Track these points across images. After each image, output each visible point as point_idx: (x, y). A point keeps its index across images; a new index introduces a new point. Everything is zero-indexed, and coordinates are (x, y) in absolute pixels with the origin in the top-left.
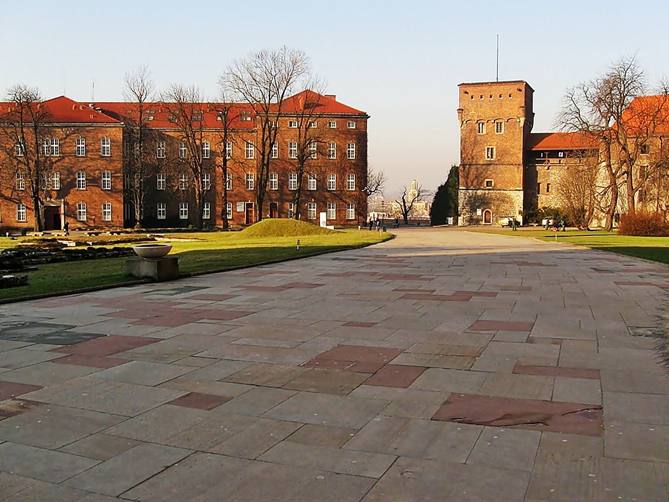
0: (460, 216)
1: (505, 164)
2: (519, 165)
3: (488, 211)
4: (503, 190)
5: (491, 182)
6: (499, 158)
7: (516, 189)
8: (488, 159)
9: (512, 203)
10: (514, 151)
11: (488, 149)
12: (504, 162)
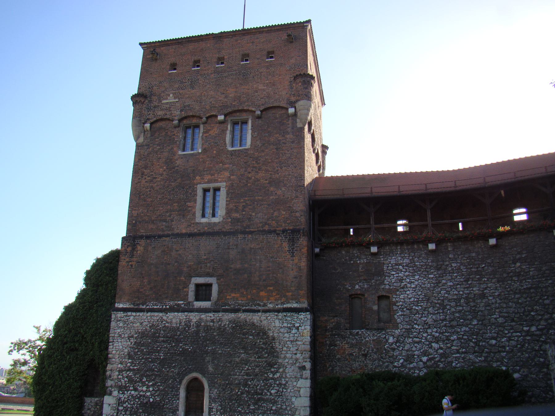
0: (110, 394)
1: (251, 233)
3: (196, 379)
4: (245, 311)
5: (210, 285)
6: (236, 215)
7: (289, 305)
8: (204, 220)
10: (279, 192)
11: (206, 191)
12: (248, 227)
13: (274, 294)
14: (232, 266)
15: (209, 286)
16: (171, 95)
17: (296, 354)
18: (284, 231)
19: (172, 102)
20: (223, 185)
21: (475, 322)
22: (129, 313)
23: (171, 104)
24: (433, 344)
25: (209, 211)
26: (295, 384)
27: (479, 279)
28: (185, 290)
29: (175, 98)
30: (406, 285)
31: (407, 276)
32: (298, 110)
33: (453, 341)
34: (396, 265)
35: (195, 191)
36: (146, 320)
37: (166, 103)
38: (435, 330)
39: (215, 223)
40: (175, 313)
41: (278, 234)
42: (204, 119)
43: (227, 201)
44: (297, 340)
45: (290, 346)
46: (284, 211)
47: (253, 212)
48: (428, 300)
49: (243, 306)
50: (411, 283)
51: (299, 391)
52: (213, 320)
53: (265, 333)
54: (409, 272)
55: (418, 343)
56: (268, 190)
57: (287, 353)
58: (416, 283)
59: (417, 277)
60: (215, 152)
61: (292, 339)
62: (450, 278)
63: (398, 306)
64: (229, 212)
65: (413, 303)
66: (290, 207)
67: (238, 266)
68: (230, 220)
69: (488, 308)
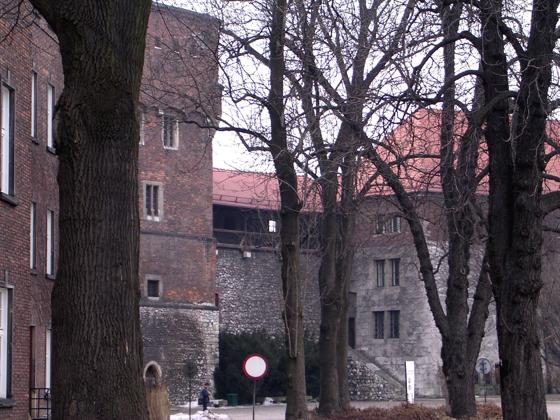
1: (183, 236)
2: (209, 240)
6: (170, 217)
7: (204, 304)
9: (201, 344)
11: (148, 187)
12: (178, 230)
13: (197, 293)
14: (172, 266)
17: (211, 345)
18: (203, 239)
21: (264, 322)
27: (269, 286)
31: (229, 277)
38: (242, 325)
41: (199, 240)
43: (164, 202)
46: (201, 218)
47: (181, 216)
48: (240, 299)
49: (179, 303)
50: (230, 284)
53: (195, 327)
56: (190, 197)
58: (233, 284)
59: (234, 279)
61: (209, 332)
62: (252, 282)
64: (166, 212)
65: (230, 301)
66: (204, 215)
67: (175, 266)
68: (166, 221)
69: (272, 310)
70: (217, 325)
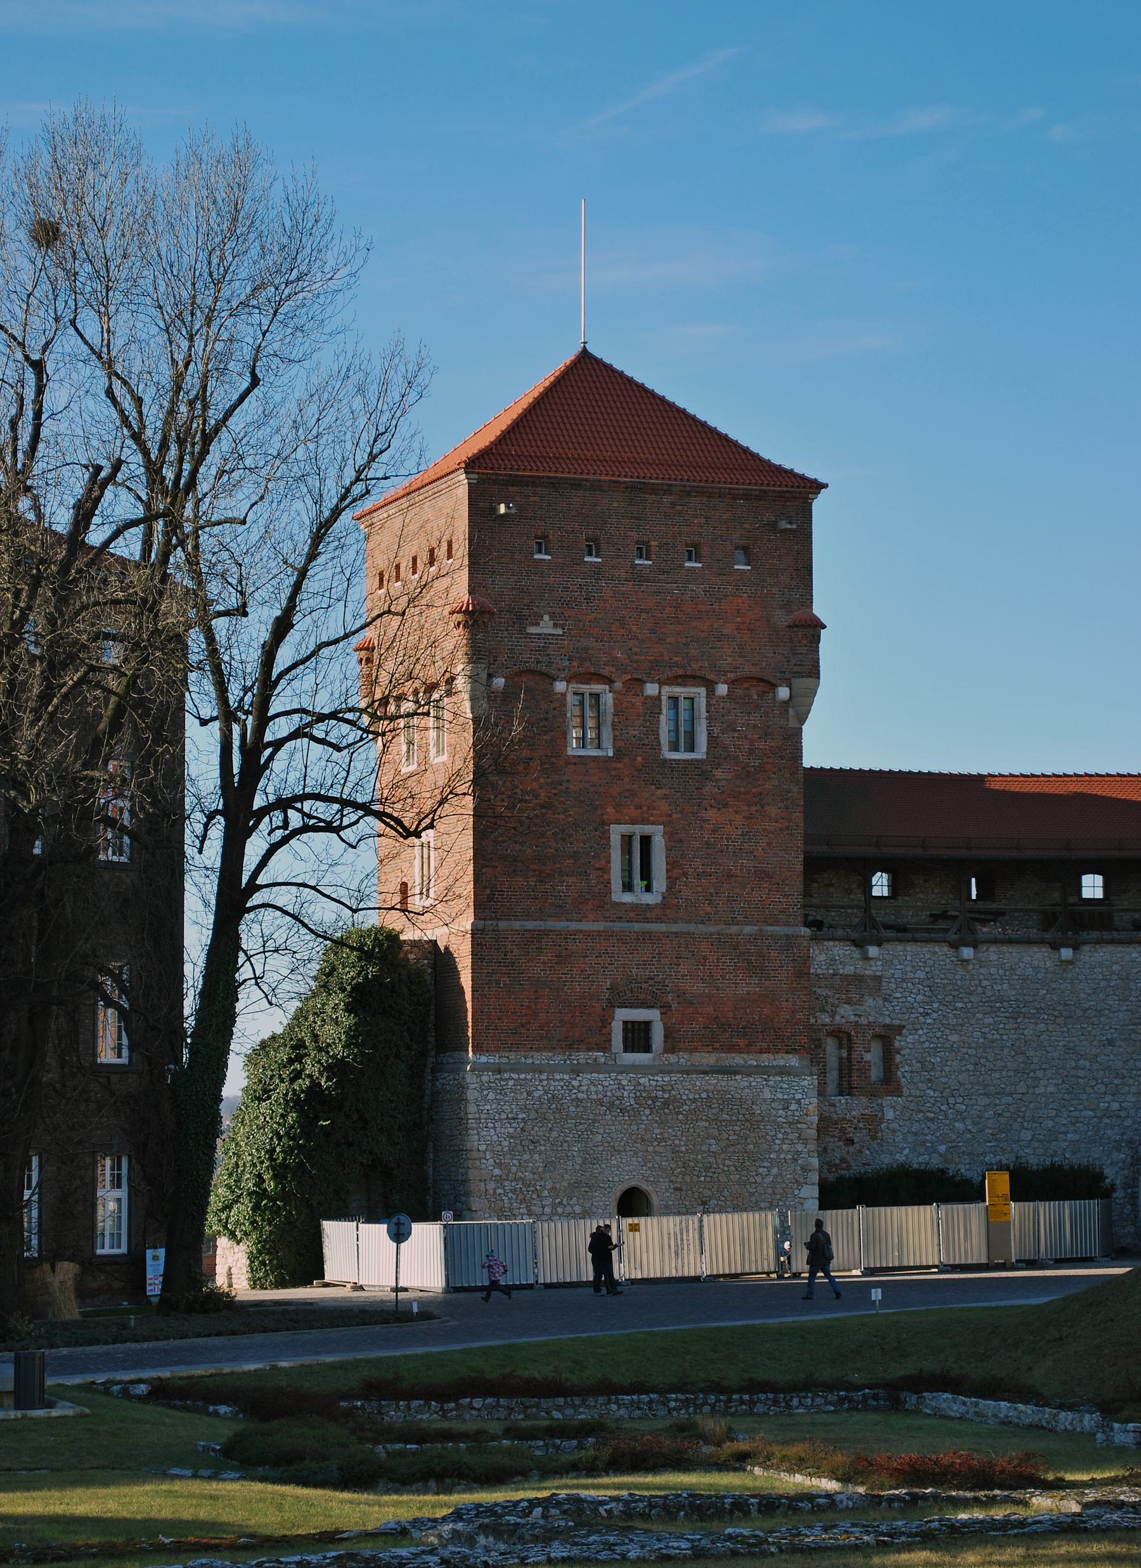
8: (627, 898)
15: (647, 1025)
16: (546, 618)
19: (549, 635)
20: (657, 833)
22: (506, 1075)
23: (548, 639)
24: (957, 1124)
25: (637, 882)
26: (796, 1192)
28: (604, 1031)
29: (555, 626)
30: (917, 1018)
32: (793, 693)
33: (988, 1119)
34: (903, 980)
35: (606, 836)
36: (539, 1087)
37: (535, 634)
38: (961, 1100)
39: (648, 905)
40: (593, 1075)
42: (618, 685)
43: (667, 864)
44: (798, 1122)
45: (788, 1130)
51: (802, 1204)
52: (661, 1086)
54: (925, 995)
55: (932, 1120)
57: (783, 1143)
59: (935, 1005)
60: (639, 759)
63: (904, 1056)
70: (812, 1103)
